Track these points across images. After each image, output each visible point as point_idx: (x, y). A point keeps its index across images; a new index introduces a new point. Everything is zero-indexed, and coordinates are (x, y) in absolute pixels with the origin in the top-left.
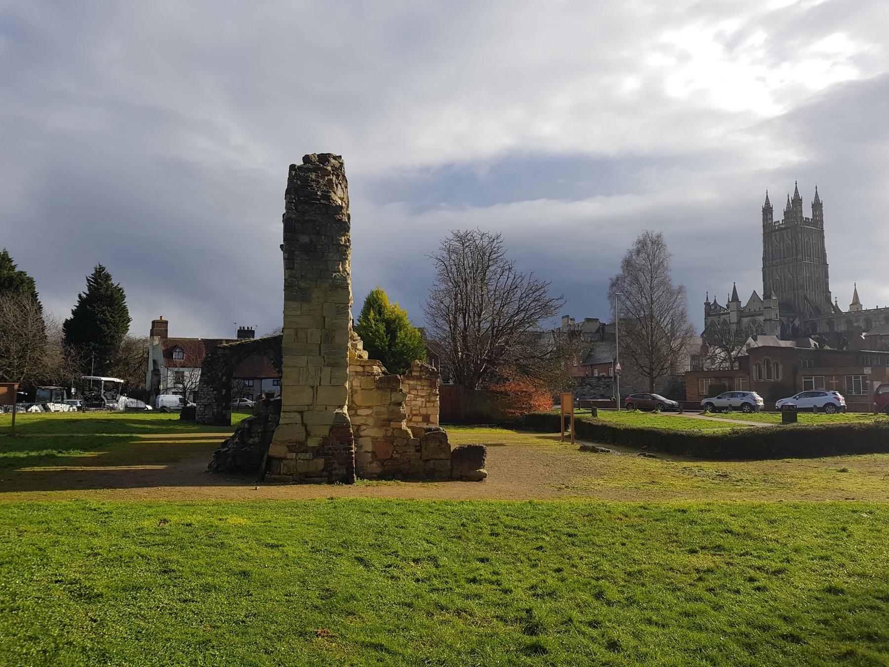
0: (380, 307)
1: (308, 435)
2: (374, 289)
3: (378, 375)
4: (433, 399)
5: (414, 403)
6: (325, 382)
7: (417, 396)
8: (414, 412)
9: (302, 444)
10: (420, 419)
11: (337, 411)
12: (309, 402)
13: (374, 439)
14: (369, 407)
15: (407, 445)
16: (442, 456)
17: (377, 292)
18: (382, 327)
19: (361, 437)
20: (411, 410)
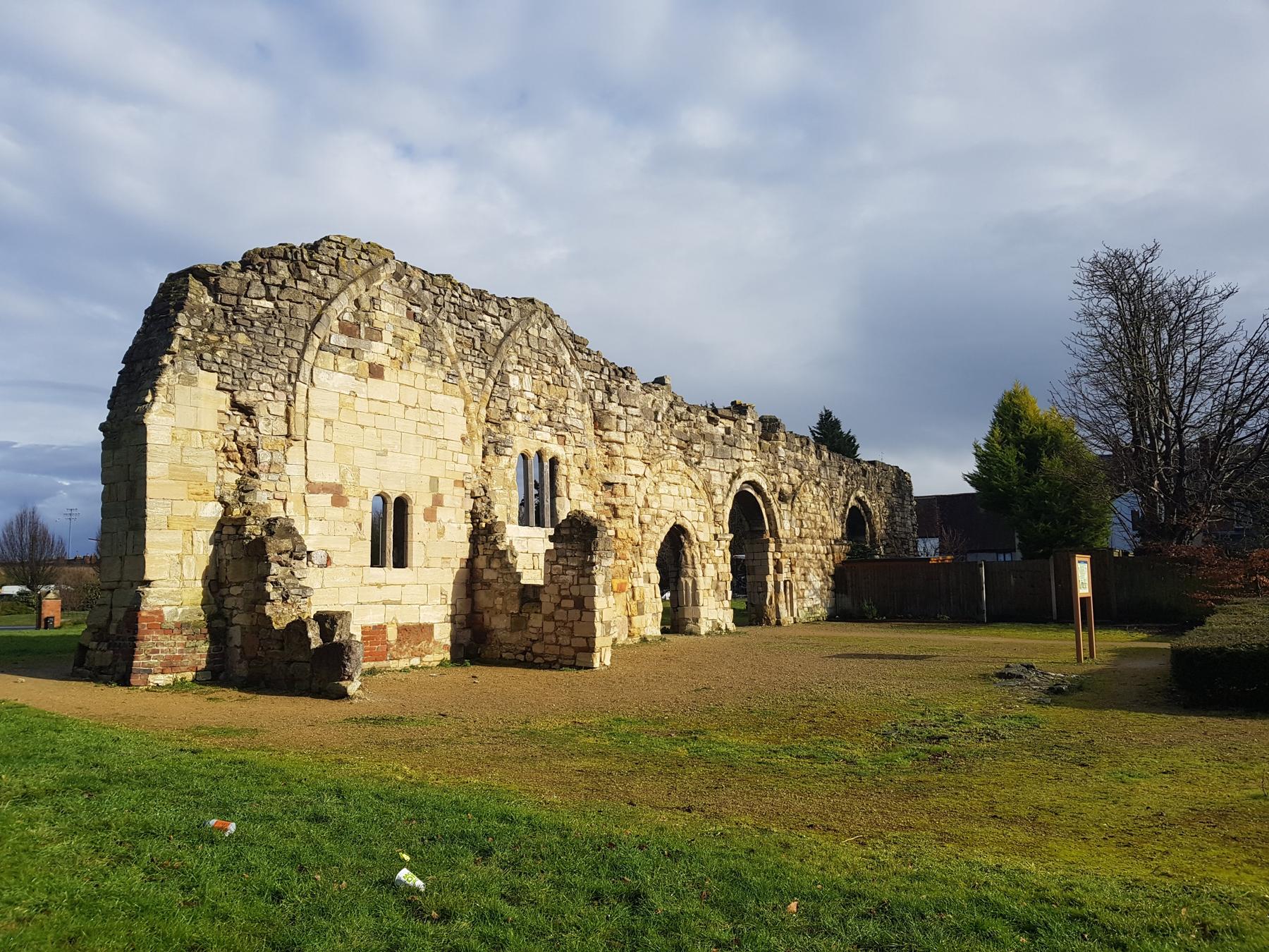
0: (1017, 418)
1: (110, 619)
2: (1010, 389)
3: (249, 538)
4: (587, 571)
5: (562, 578)
6: (129, 552)
7: (566, 567)
8: (563, 593)
9: (106, 629)
10: (570, 603)
11: (140, 588)
12: (117, 576)
13: (243, 628)
14: (238, 584)
15: (270, 638)
16: (301, 657)
17: (1011, 396)
18: (1010, 456)
19: (233, 625)
20: (560, 590)
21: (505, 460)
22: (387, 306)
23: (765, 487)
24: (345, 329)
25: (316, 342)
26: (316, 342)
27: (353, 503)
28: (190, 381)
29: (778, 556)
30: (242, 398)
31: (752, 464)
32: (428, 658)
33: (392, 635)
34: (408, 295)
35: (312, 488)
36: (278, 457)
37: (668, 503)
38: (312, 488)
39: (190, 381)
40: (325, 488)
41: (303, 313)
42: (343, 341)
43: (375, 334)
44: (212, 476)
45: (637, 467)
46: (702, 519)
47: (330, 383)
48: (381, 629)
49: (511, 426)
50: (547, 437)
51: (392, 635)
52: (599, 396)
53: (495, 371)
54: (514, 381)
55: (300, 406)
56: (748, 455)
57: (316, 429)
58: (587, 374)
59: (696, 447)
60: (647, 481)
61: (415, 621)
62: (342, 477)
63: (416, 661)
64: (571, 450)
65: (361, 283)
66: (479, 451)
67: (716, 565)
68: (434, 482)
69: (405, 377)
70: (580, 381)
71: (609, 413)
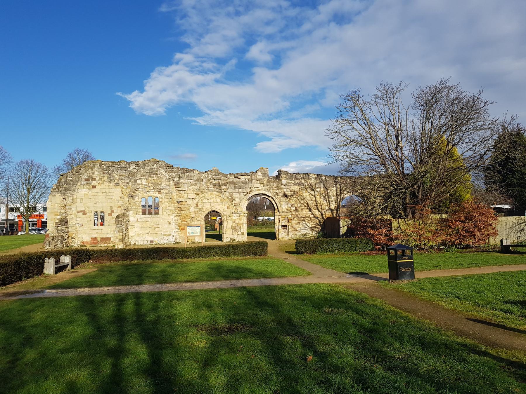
21: (136, 200)
22: (97, 173)
23: (270, 195)
24: (86, 180)
25: (79, 184)
26: (79, 184)
27: (88, 214)
28: (54, 195)
29: (280, 217)
30: (64, 197)
31: (260, 188)
32: (109, 244)
33: (99, 239)
34: (103, 169)
35: (78, 212)
36: (70, 207)
37: (208, 205)
38: (78, 212)
39: (54, 195)
40: (81, 212)
41: (77, 179)
42: (85, 182)
43: (94, 179)
44: (59, 211)
45: (194, 196)
46: (226, 208)
47: (81, 191)
48: (96, 238)
49: (137, 192)
50: (153, 193)
51: (99, 239)
52: (176, 179)
53: (132, 180)
54: (139, 181)
55: (75, 197)
56: (259, 185)
57: (78, 200)
58: (171, 174)
59: (223, 187)
60: (197, 200)
61: (105, 237)
62: (85, 209)
63: (106, 245)
64: (163, 195)
65: (90, 170)
66: (126, 199)
67: (234, 221)
68: (111, 208)
69: (102, 187)
70: (167, 176)
71: (179, 183)
